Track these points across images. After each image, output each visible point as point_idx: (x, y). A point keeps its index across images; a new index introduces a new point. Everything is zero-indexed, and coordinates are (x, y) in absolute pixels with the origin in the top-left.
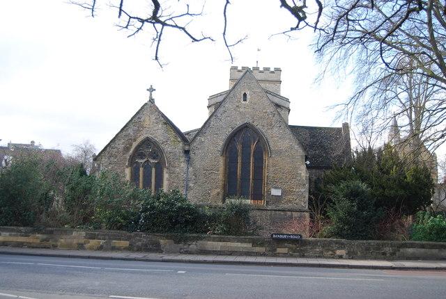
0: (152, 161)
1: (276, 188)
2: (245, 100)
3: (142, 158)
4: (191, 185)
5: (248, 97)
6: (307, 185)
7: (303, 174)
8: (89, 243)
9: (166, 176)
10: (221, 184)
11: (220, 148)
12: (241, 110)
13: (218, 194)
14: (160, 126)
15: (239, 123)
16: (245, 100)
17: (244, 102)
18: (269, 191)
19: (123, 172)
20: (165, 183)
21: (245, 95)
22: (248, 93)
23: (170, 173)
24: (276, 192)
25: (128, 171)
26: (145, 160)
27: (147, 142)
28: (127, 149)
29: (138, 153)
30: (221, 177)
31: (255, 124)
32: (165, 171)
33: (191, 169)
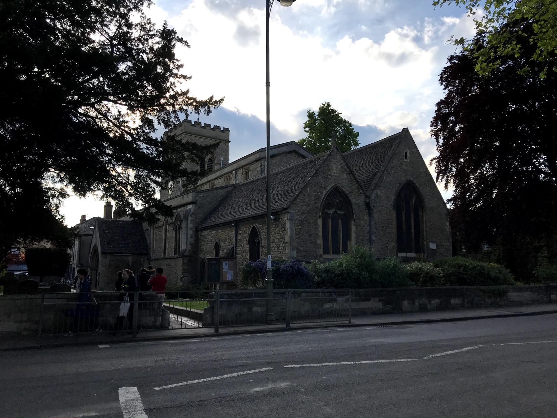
0: (339, 212)
1: (433, 242)
2: (406, 158)
3: (329, 209)
4: (374, 238)
5: (408, 155)
6: (451, 240)
7: (448, 230)
8: (335, 300)
9: (353, 228)
10: (395, 237)
11: (392, 203)
12: (405, 167)
13: (394, 246)
14: (345, 175)
15: (404, 179)
16: (406, 158)
17: (405, 160)
18: (428, 245)
19: (316, 223)
20: (353, 235)
21: (406, 153)
22: (408, 152)
23: (357, 226)
24: (433, 246)
25: (320, 222)
26: (334, 210)
27: (336, 191)
28: (318, 198)
29: (327, 204)
30: (394, 231)
31: (415, 181)
32: (352, 223)
33: (373, 223)
